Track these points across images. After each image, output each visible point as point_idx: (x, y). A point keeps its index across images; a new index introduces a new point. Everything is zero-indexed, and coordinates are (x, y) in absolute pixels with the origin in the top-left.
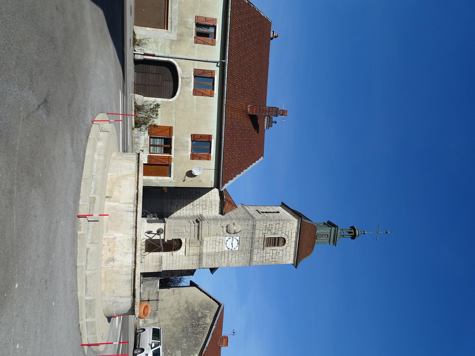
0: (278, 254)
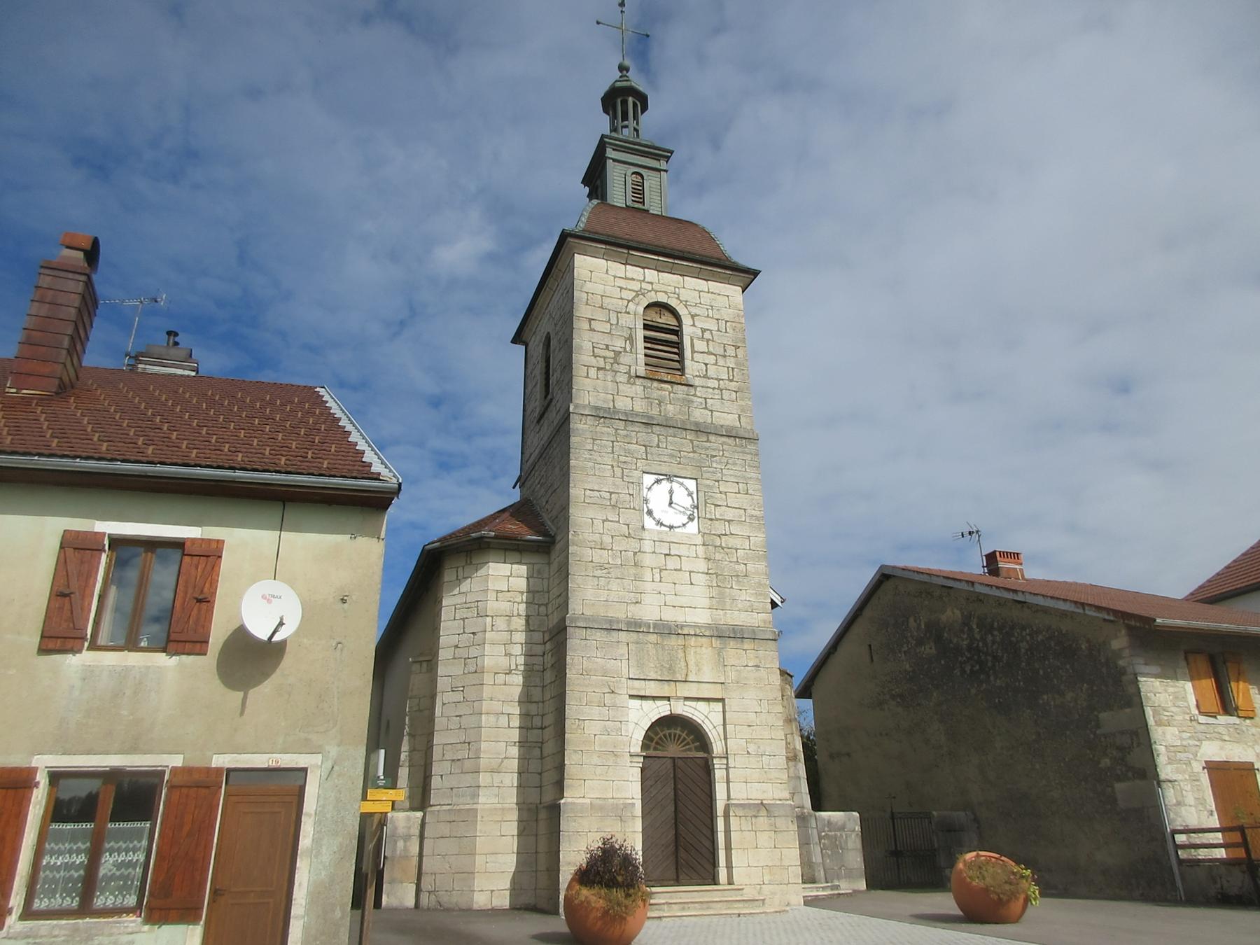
0: (707, 335)
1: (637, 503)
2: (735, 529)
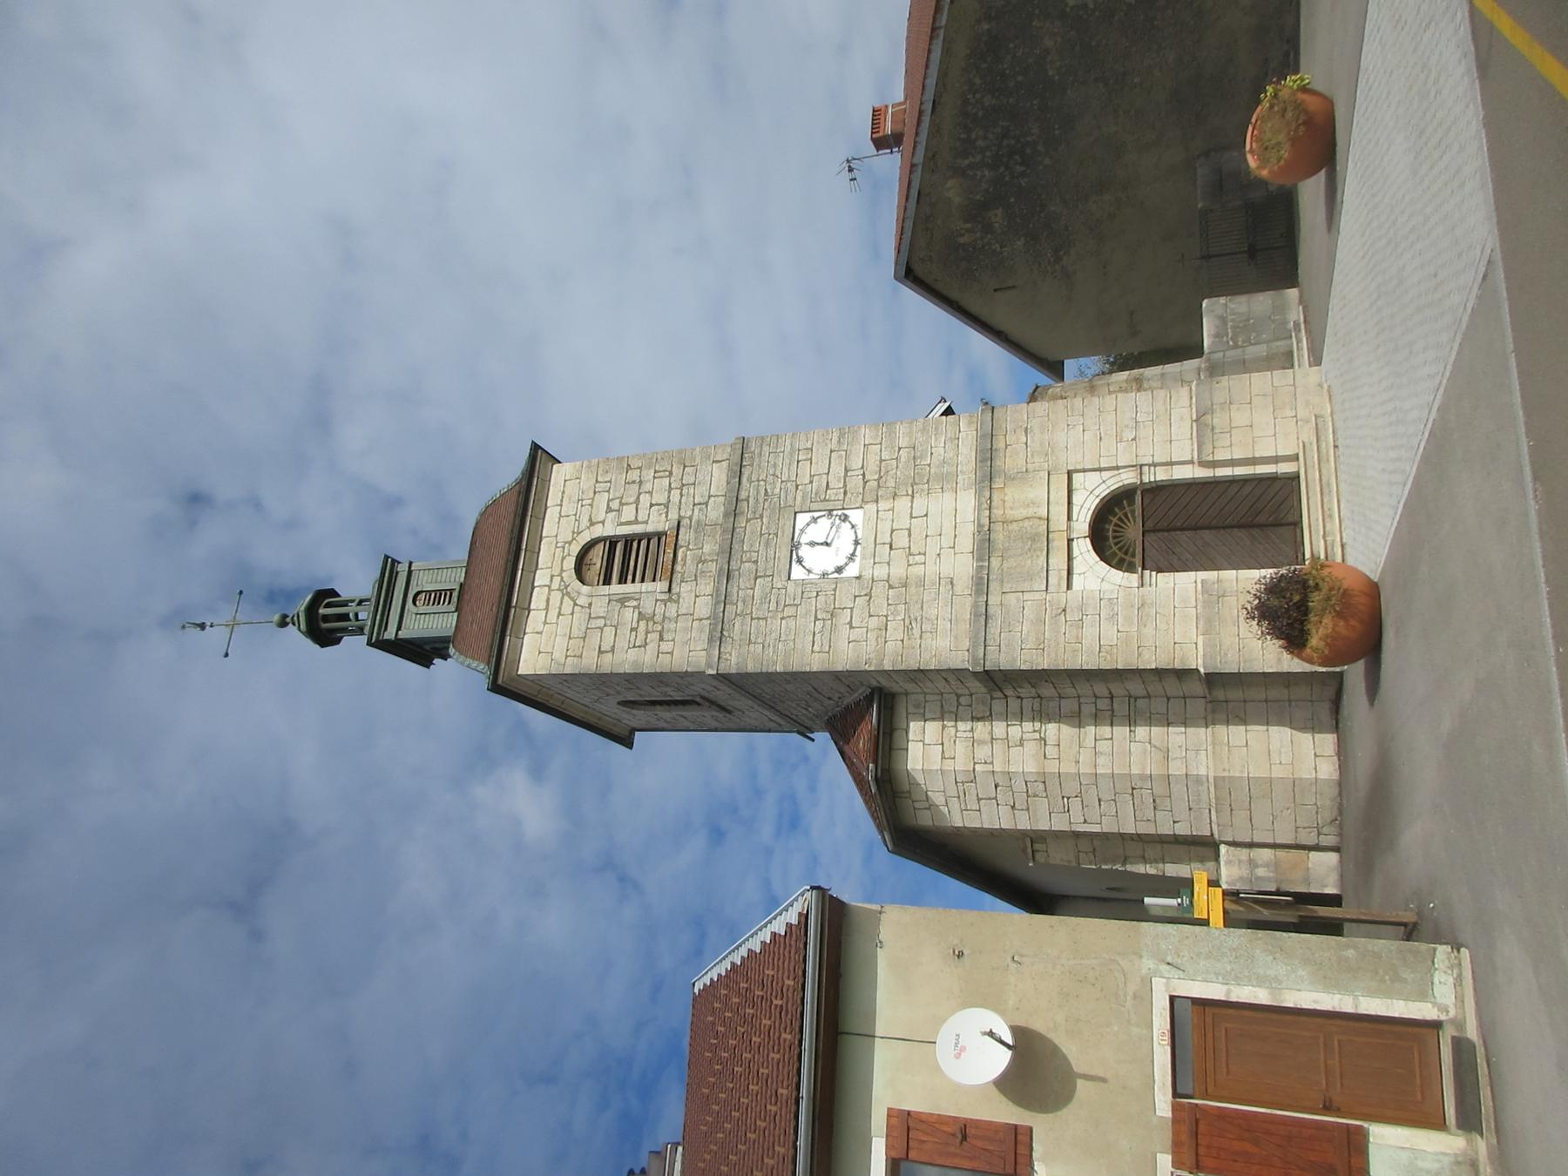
2: (856, 463)
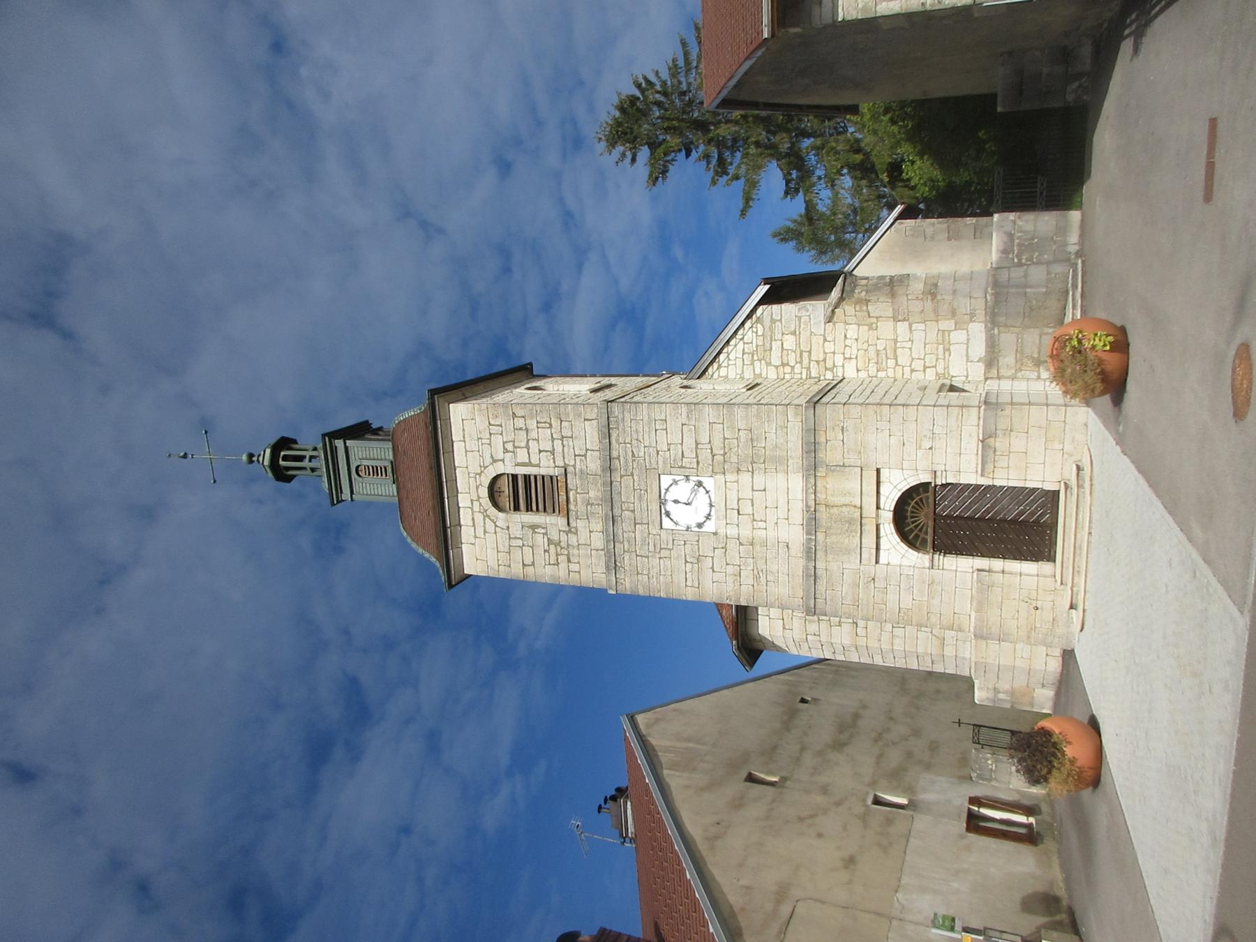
0: (510, 447)
1: (691, 537)
